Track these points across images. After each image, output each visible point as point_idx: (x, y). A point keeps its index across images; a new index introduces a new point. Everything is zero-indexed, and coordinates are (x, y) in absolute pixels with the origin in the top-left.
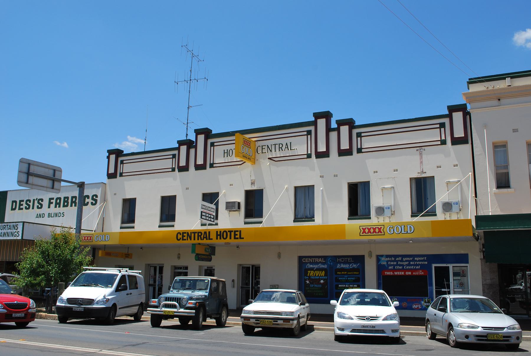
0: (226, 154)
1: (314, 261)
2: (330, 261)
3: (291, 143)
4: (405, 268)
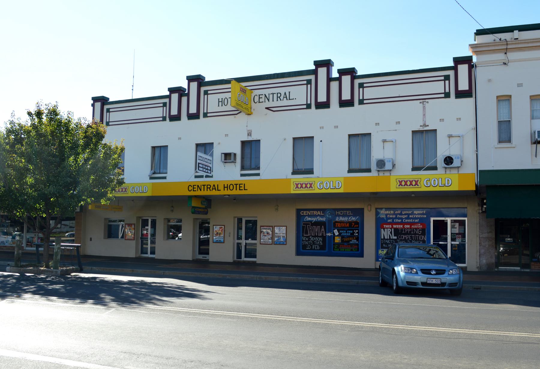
0: (220, 103)
1: (312, 214)
2: (329, 214)
3: (289, 92)
4: (404, 221)
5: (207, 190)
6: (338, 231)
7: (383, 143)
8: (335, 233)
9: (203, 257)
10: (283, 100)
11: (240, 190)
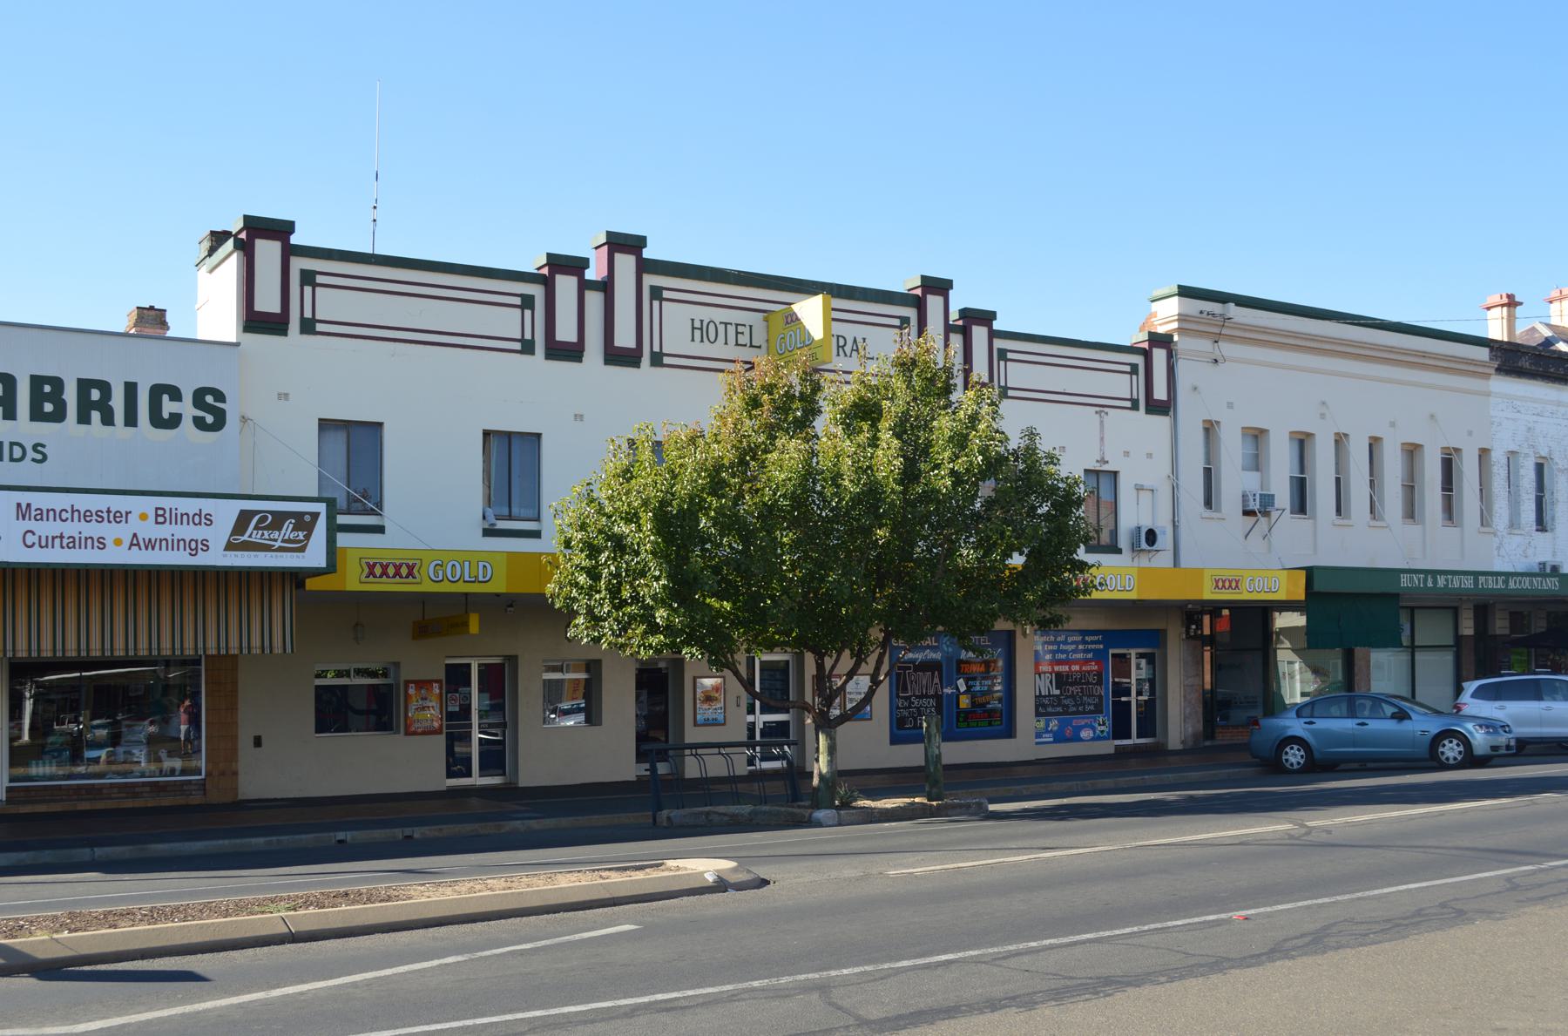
0: (697, 333)
2: (948, 643)
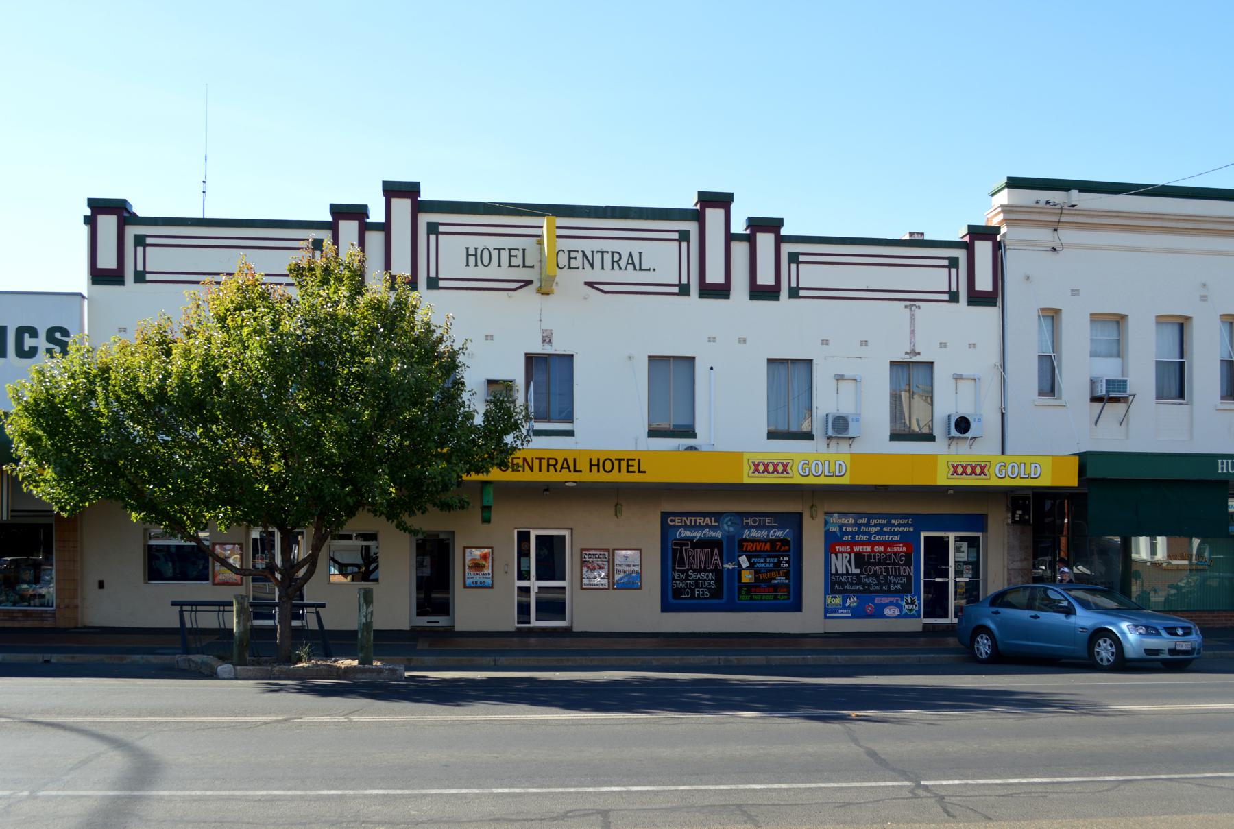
0: (472, 259)
1: (693, 524)
2: (729, 523)
3: (640, 253)
4: (872, 539)
5: (548, 471)
6: (749, 559)
7: (836, 381)
8: (741, 563)
9: (428, 622)
10: (626, 269)
11: (628, 472)
